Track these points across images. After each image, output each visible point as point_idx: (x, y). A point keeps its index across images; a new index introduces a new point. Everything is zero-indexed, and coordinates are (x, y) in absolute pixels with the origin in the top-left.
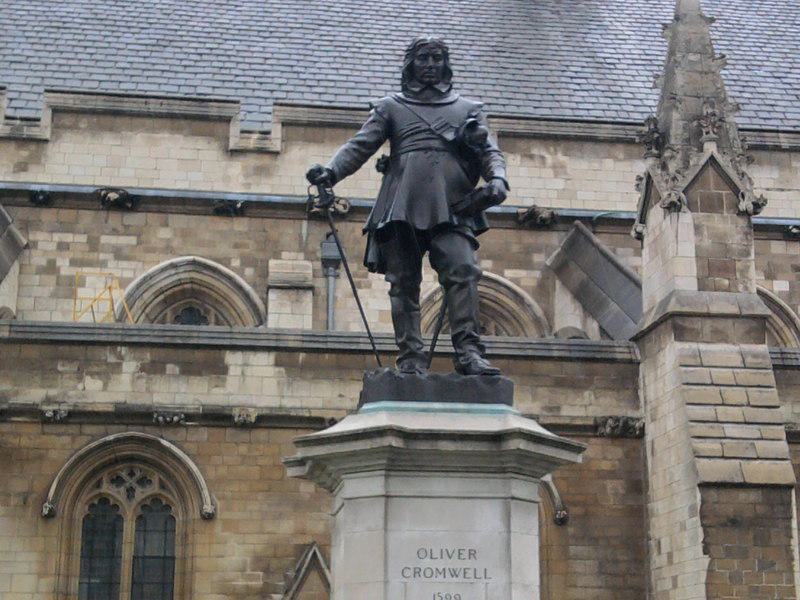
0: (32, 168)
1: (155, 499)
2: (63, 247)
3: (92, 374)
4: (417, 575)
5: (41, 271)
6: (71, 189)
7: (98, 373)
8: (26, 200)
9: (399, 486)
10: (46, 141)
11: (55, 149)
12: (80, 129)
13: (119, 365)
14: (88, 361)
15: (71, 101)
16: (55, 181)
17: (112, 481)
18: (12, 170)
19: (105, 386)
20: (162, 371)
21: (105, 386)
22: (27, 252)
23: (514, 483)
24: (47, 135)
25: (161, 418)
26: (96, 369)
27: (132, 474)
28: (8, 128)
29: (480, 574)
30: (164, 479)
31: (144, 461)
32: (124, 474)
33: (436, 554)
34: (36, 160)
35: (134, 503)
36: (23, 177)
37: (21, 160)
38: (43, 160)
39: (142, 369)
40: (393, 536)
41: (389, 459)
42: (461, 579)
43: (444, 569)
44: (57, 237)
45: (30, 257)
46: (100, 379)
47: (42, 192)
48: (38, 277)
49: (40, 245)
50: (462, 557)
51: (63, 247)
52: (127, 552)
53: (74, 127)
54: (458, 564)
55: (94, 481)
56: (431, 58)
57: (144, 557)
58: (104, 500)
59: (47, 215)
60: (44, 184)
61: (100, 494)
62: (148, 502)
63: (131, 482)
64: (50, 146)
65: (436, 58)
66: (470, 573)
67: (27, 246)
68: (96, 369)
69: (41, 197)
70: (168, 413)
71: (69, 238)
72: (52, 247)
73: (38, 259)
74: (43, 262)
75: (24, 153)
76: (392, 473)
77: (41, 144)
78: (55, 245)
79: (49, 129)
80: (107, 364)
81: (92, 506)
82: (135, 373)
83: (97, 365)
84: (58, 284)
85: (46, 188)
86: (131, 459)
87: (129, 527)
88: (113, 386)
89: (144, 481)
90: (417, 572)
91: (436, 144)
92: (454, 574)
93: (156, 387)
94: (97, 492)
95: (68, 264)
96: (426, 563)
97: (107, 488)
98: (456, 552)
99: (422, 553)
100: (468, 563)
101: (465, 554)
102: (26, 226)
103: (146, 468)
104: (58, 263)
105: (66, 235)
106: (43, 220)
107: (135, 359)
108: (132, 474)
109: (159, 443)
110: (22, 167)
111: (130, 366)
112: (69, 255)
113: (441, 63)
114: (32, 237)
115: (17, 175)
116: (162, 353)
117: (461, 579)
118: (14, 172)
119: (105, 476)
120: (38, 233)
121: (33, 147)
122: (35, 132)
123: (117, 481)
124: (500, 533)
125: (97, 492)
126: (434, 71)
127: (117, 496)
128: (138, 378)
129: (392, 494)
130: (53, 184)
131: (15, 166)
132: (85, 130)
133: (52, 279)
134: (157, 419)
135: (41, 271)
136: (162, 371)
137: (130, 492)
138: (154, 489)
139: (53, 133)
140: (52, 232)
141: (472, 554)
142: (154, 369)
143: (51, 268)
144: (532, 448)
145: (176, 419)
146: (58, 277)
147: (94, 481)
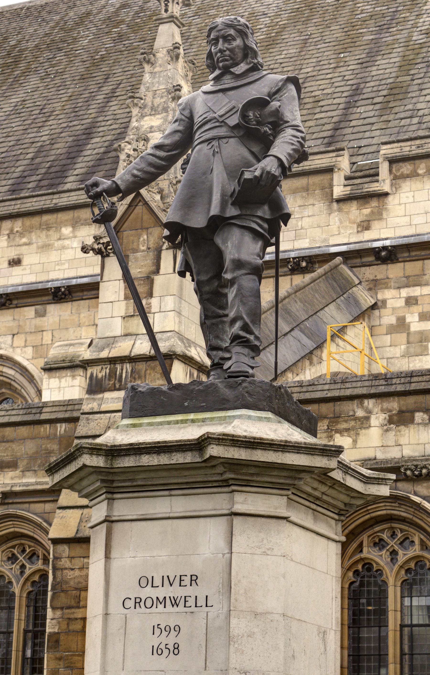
0: (375, 225)
1: (419, 560)
2: (411, 301)
3: (340, 432)
4: (137, 605)
5: (392, 330)
6: (412, 240)
7: (347, 430)
8: (371, 259)
9: (125, 508)
10: (386, 194)
11: (396, 201)
12: (418, 175)
13: (368, 418)
14: (336, 418)
15: (408, 149)
16: (398, 235)
17: (375, 544)
18: (355, 231)
19: (355, 442)
20: (412, 421)
21: (355, 442)
22: (376, 312)
23: (238, 497)
24: (386, 187)
25: (409, 473)
26: (344, 426)
27: (393, 535)
28: (349, 188)
29: (201, 602)
30: (425, 539)
31: (403, 520)
32: (385, 536)
33: (158, 582)
34: (378, 215)
35: (396, 567)
36: (367, 235)
37: (365, 218)
38: (385, 216)
39: (390, 421)
40: (115, 564)
41: (103, 481)
42: (181, 607)
43: (165, 598)
44: (405, 292)
45: (380, 317)
46: (349, 436)
47: (384, 248)
48: (389, 336)
49: (390, 303)
50: (183, 583)
51: (411, 301)
52: (393, 620)
53: (414, 175)
54: (176, 591)
55: (354, 545)
56: (221, 41)
57: (412, 626)
58: (368, 565)
59: (394, 271)
60: (386, 239)
61: (362, 559)
62: (412, 565)
63: (393, 544)
64: (390, 198)
65: (227, 39)
66: (191, 602)
67: (374, 307)
68: (344, 426)
69: (383, 254)
70: (416, 466)
71: (416, 291)
72: (401, 303)
73: (388, 318)
74: (393, 320)
75: (367, 211)
76: (116, 496)
77: (381, 199)
78: (404, 300)
79: (388, 182)
80: (356, 419)
81: (356, 573)
82: (382, 426)
83: (346, 421)
84: (408, 342)
85: (387, 243)
86: (390, 518)
87: (393, 593)
88: (362, 441)
89: (405, 542)
90: (138, 602)
91: (222, 131)
92: (175, 603)
93: (403, 440)
94: (357, 557)
95: (417, 318)
96: (148, 592)
97: (369, 553)
98: (178, 579)
99: (146, 581)
100: (189, 591)
101: (187, 581)
102: (375, 285)
103: (406, 528)
104: (408, 320)
105: (412, 289)
106: (391, 276)
107: (382, 410)
108: (393, 535)
109: (409, 498)
110: (365, 226)
111: (378, 419)
112: (417, 309)
113: (238, 42)
114: (380, 296)
115: (360, 235)
116: (411, 400)
117: (181, 607)
118: (358, 232)
119: (365, 538)
120: (386, 291)
121: (374, 203)
122: (374, 187)
123: (379, 544)
124: (224, 555)
125: (357, 557)
126: (227, 53)
127: (377, 559)
128: (387, 431)
129: (114, 518)
130: (395, 238)
131: (358, 226)
132: (423, 176)
133: (403, 337)
134: (405, 474)
135: (392, 330)
136: (412, 421)
137: (394, 553)
138: (415, 550)
139: (392, 185)
140: (399, 288)
141: (194, 579)
142: (401, 419)
143: (401, 325)
144: (242, 454)
145: (424, 471)
146: (408, 334)
147: (354, 545)
